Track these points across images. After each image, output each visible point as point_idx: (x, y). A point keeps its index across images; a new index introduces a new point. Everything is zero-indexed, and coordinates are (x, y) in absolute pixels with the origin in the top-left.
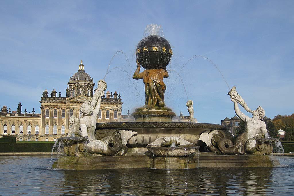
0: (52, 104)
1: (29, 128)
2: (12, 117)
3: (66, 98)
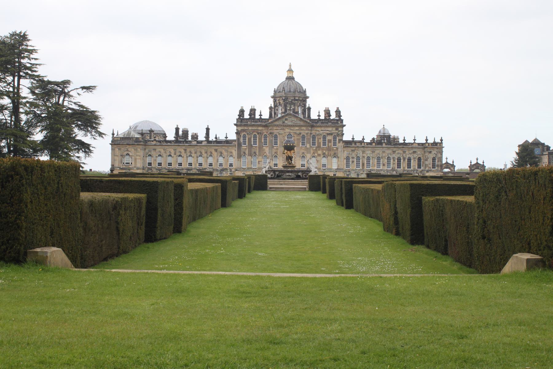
0: (250, 128)
1: (221, 160)
3: (268, 120)
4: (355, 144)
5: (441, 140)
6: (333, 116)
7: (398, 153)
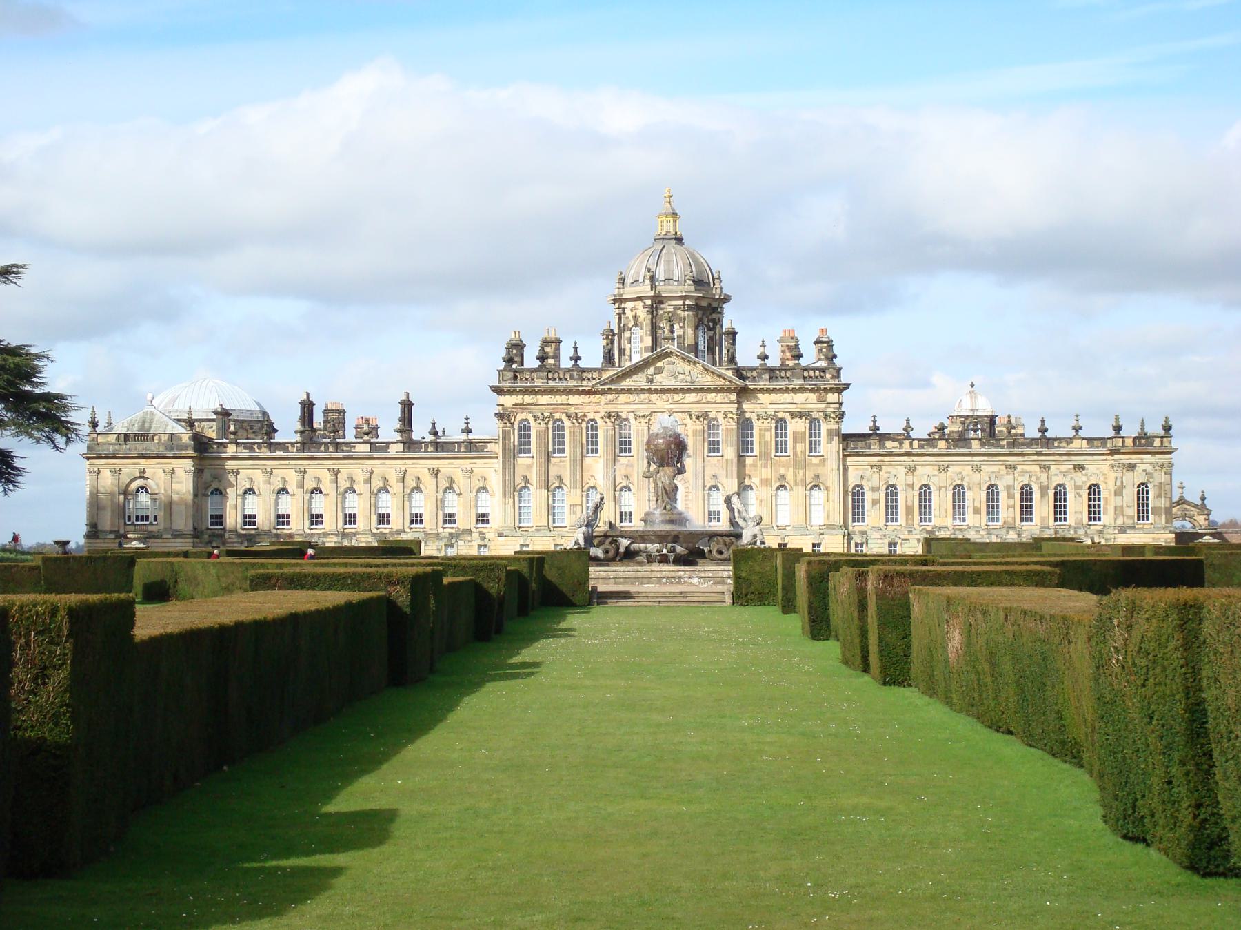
0: (544, 399)
2: (376, 454)
3: (599, 371)
4: (882, 446)
5: (1167, 428)
6: (810, 356)
7: (1023, 472)
